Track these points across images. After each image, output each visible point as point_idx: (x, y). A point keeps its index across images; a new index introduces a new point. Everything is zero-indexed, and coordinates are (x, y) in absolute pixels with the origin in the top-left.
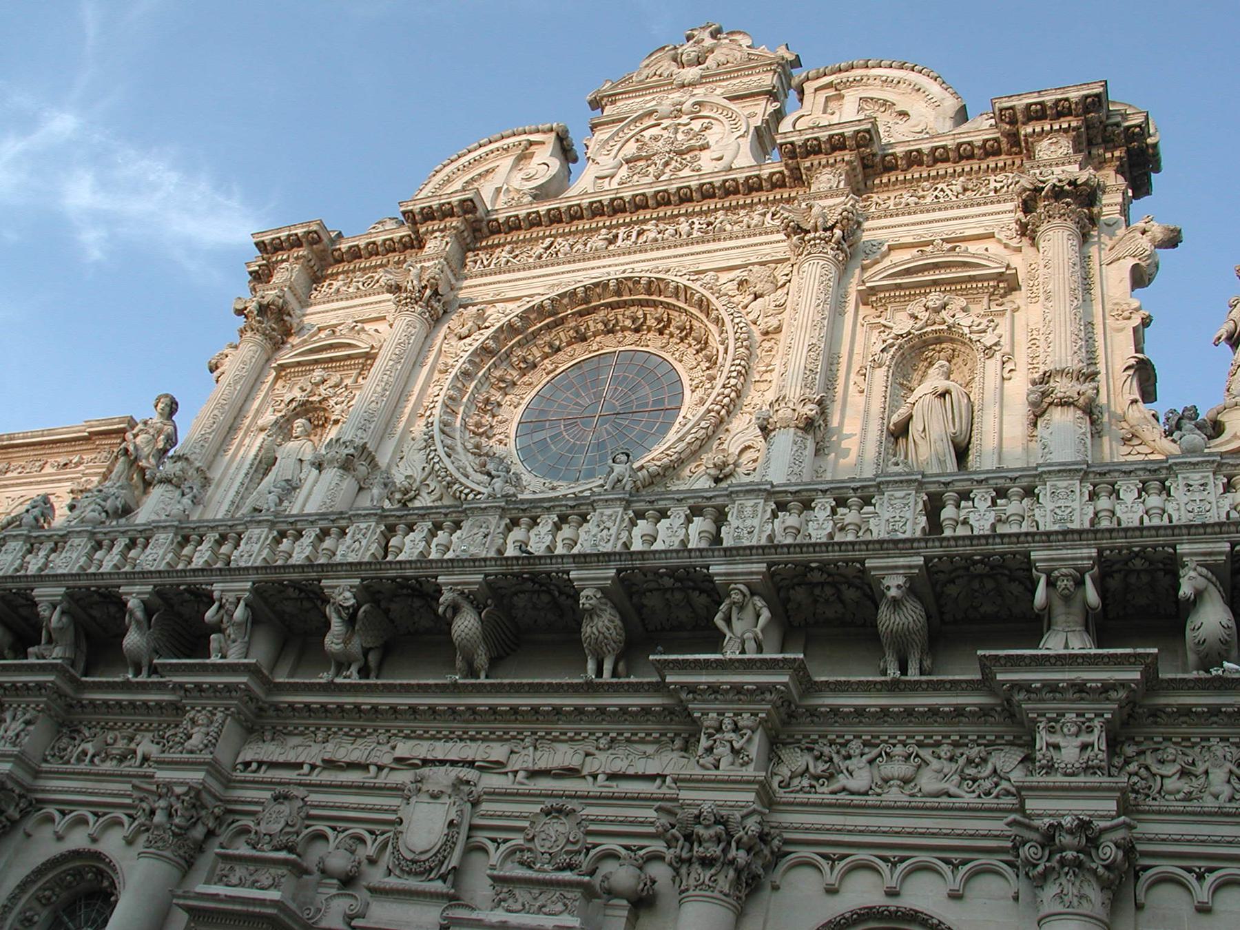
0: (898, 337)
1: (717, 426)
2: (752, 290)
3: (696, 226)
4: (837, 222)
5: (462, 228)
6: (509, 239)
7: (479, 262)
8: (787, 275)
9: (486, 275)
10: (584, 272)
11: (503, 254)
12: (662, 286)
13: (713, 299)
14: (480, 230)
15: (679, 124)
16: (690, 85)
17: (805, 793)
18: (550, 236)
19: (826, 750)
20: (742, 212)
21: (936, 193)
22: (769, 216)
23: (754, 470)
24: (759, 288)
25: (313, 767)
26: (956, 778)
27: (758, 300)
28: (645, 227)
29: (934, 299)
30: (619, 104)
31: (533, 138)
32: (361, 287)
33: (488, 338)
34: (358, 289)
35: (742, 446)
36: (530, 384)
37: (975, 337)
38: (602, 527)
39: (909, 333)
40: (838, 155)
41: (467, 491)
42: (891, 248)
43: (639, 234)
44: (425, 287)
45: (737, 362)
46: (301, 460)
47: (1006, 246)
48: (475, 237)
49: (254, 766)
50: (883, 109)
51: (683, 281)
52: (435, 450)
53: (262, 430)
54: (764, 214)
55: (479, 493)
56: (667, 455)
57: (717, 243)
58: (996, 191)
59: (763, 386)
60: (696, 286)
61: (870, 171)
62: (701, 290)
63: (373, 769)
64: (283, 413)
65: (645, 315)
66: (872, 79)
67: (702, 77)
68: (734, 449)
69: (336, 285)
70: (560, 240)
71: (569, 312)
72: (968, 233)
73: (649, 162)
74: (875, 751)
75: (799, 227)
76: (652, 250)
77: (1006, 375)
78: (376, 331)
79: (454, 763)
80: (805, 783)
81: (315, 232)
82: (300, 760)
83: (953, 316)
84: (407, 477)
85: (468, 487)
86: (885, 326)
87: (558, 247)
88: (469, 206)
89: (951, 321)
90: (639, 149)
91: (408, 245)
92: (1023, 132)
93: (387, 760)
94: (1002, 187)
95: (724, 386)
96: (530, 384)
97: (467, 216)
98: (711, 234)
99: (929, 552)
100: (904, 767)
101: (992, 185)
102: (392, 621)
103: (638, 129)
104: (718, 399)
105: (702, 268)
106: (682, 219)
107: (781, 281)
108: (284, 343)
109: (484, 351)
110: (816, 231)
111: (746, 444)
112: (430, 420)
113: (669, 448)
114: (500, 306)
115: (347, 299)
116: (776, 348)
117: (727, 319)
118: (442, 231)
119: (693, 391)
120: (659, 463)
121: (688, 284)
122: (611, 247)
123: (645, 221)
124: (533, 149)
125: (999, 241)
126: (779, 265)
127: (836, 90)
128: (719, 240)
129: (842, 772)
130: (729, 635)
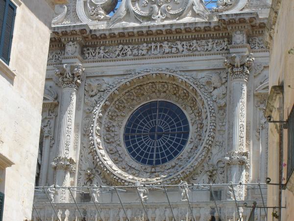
1: (207, 153)
2: (213, 86)
3: (185, 47)
5: (81, 39)
6: (102, 43)
7: (90, 54)
8: (225, 78)
18: (120, 43)
20: (204, 42)
22: (215, 45)
24: (215, 85)
27: (216, 90)
33: (106, 101)
36: (124, 116)
42: (264, 67)
43: (161, 46)
45: (212, 124)
51: (184, 79)
52: (99, 158)
56: (192, 167)
59: (222, 132)
62: (192, 84)
68: (215, 162)
70: (126, 47)
71: (136, 85)
75: (230, 64)
85: (116, 176)
87: (126, 51)
96: (124, 116)
98: (192, 52)
104: (208, 142)
106: (179, 43)
107: (224, 80)
110: (237, 67)
113: (192, 164)
114: (106, 79)
116: (225, 114)
120: (189, 170)
121: (187, 80)
123: (161, 42)
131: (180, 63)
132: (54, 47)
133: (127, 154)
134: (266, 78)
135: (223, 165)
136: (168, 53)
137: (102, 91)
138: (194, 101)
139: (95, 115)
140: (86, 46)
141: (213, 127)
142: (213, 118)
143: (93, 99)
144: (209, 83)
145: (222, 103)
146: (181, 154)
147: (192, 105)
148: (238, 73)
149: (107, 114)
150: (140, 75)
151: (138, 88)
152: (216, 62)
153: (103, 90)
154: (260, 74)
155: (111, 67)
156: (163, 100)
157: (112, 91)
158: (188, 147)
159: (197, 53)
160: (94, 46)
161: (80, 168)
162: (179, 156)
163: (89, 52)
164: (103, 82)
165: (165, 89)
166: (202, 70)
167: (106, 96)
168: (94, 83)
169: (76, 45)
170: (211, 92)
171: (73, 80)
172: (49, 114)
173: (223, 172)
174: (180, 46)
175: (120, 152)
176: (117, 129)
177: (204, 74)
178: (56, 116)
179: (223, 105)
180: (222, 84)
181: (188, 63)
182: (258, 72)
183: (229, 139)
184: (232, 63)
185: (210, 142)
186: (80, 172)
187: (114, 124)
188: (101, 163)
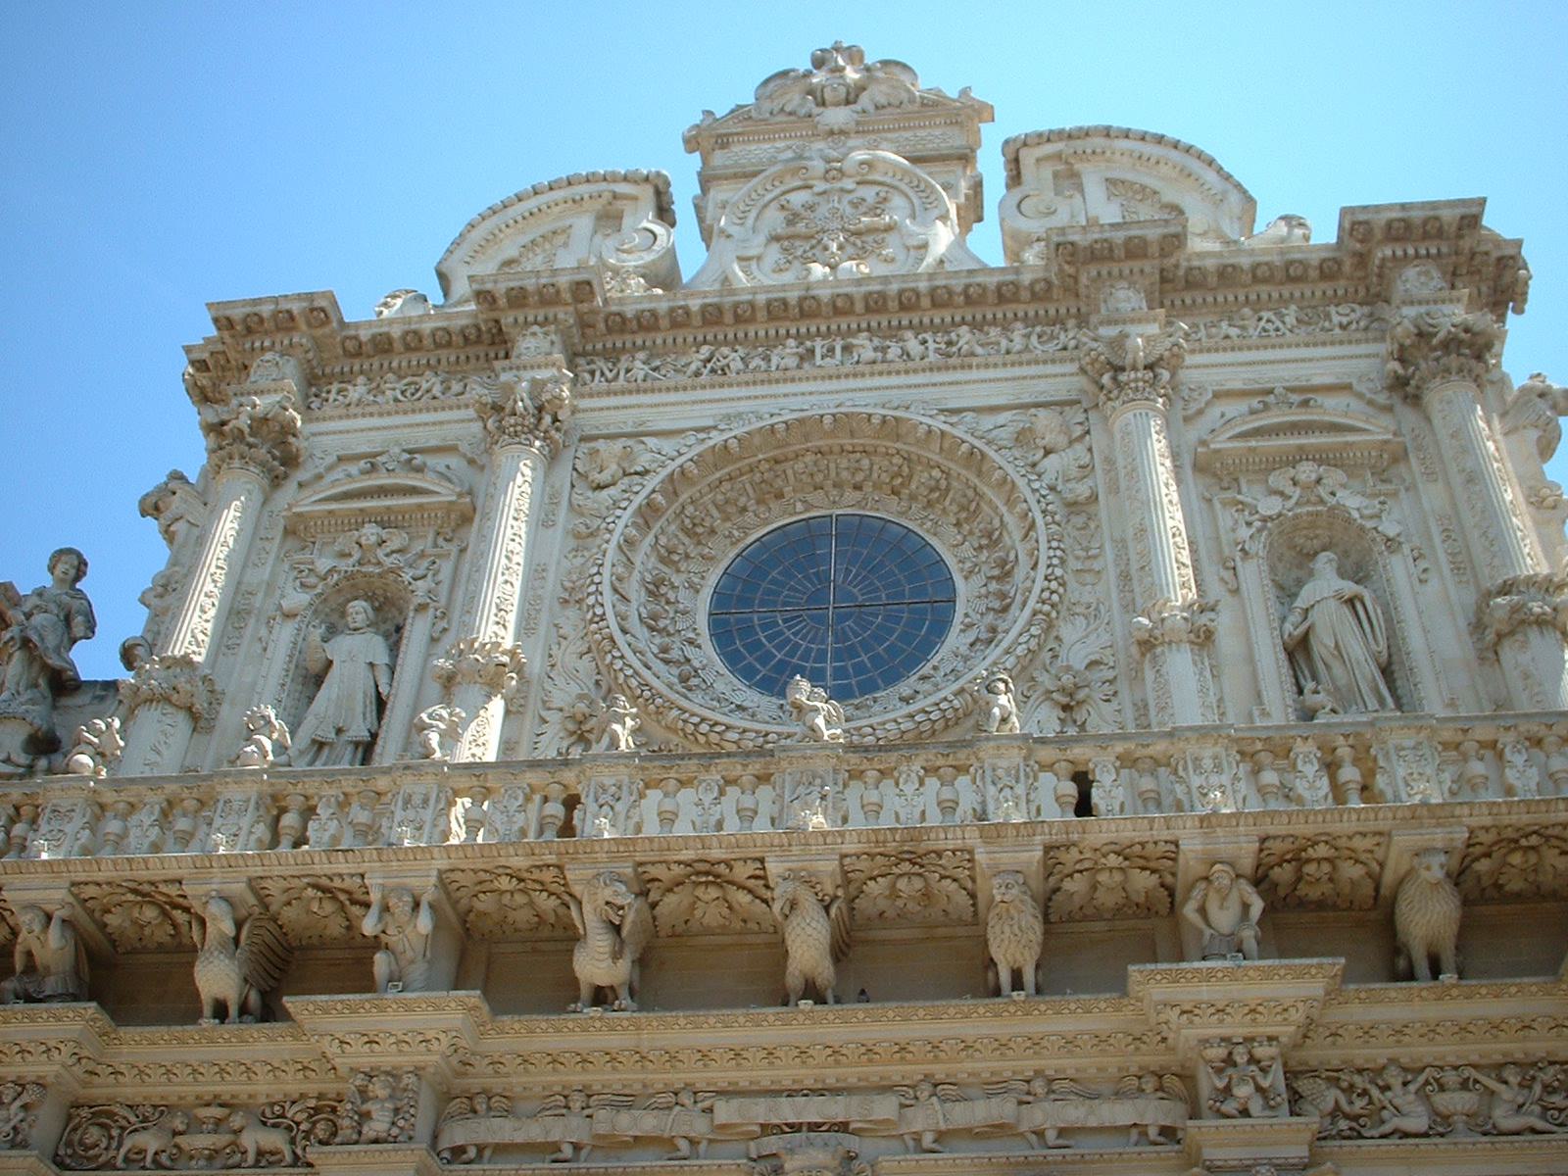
0: (1264, 520)
3: (931, 345)
4: (1161, 358)
8: (1081, 424)
9: (615, 394)
10: (773, 400)
11: (638, 364)
12: (903, 430)
13: (990, 452)
14: (592, 326)
15: (842, 190)
16: (842, 132)
17: (1344, 1138)
19: (1359, 1081)
20: (994, 332)
21: (1262, 323)
22: (1034, 339)
23: (1115, 693)
24: (1049, 439)
25: (577, 1147)
26: (1537, 1109)
28: (855, 341)
29: (1307, 471)
30: (735, 149)
31: (622, 188)
32: (400, 397)
33: (654, 491)
34: (396, 400)
35: (1087, 661)
37: (1369, 524)
38: (1000, 786)
39: (1280, 515)
40: (1136, 265)
41: (696, 720)
42: (1217, 395)
43: (847, 349)
44: (540, 409)
45: (1054, 544)
46: (371, 664)
47: (1370, 403)
48: (583, 335)
49: (472, 1153)
50: (1139, 197)
51: (938, 424)
52: (622, 657)
53: (289, 616)
54: (1028, 336)
55: (716, 724)
57: (967, 371)
58: (1343, 327)
59: (1089, 578)
60: (958, 432)
61: (1168, 286)
62: (968, 438)
63: (683, 1145)
64: (318, 590)
65: (872, 465)
66: (1118, 154)
67: (858, 123)
68: (1079, 665)
69: (357, 391)
70: (725, 350)
71: (761, 456)
72: (1316, 381)
73: (814, 242)
74: (1421, 1079)
75: (1109, 363)
76: (872, 374)
77: (1423, 576)
78: (448, 467)
79: (814, 1127)
80: (1343, 1124)
81: (323, 310)
82: (555, 1137)
83: (1333, 494)
84: (581, 697)
85: (693, 715)
86: (1241, 503)
87: (724, 362)
88: (583, 289)
89: (1332, 501)
90: (790, 223)
91: (473, 337)
92: (1380, 255)
93: (700, 1127)
94: (1350, 323)
95: (1046, 578)
97: (580, 306)
98: (952, 358)
99: (1474, 822)
100: (1466, 1095)
101: (1336, 319)
102: (654, 918)
103: (777, 192)
104: (1046, 594)
105: (951, 405)
106: (909, 334)
107: (1078, 431)
108: (286, 476)
109: (648, 514)
110: (1134, 368)
111: (1093, 658)
112: (599, 611)
114: (651, 442)
115: (381, 415)
116: (1092, 525)
117: (1021, 483)
118: (541, 325)
119: (966, 578)
121: (946, 428)
122: (806, 365)
123: (850, 333)
124: (619, 204)
125: (1360, 396)
126: (1067, 408)
127: (1067, 163)
128: (970, 367)
129: (1384, 1108)
130: (1208, 932)
131: (915, 391)
132: (473, 361)
133: (724, 670)
134: (1226, 418)
135: (1110, 674)
136: (874, 362)
137: (636, 473)
138: (970, 509)
139: (610, 532)
140: (584, 354)
141: (1059, 553)
142: (1054, 527)
143: (605, 493)
144: (1023, 438)
145: (1082, 490)
146: (934, 662)
147: (964, 515)
148: (1141, 384)
149: (650, 539)
150: (775, 420)
151: (764, 466)
152: (1042, 385)
153: (639, 469)
154: (1200, 412)
155: (668, 409)
156: (849, 511)
157: (672, 466)
158: (955, 639)
159: (975, 361)
160: (612, 355)
161: (544, 702)
162: (927, 670)
163: (593, 366)
164: (642, 446)
165: (860, 477)
166: (993, 410)
167: (652, 482)
168: (610, 450)
169: (553, 337)
170: (1034, 465)
171: (536, 427)
172: (435, 545)
173: (1115, 693)
174: (913, 345)
175: (696, 663)
176: (683, 595)
177: (1003, 418)
178: (463, 551)
179: (1087, 493)
180: (1071, 443)
181: (943, 388)
182: (1194, 407)
183: (1125, 577)
184: (1118, 362)
185: (1055, 597)
186: (544, 713)
187: (676, 580)
188: (630, 672)
